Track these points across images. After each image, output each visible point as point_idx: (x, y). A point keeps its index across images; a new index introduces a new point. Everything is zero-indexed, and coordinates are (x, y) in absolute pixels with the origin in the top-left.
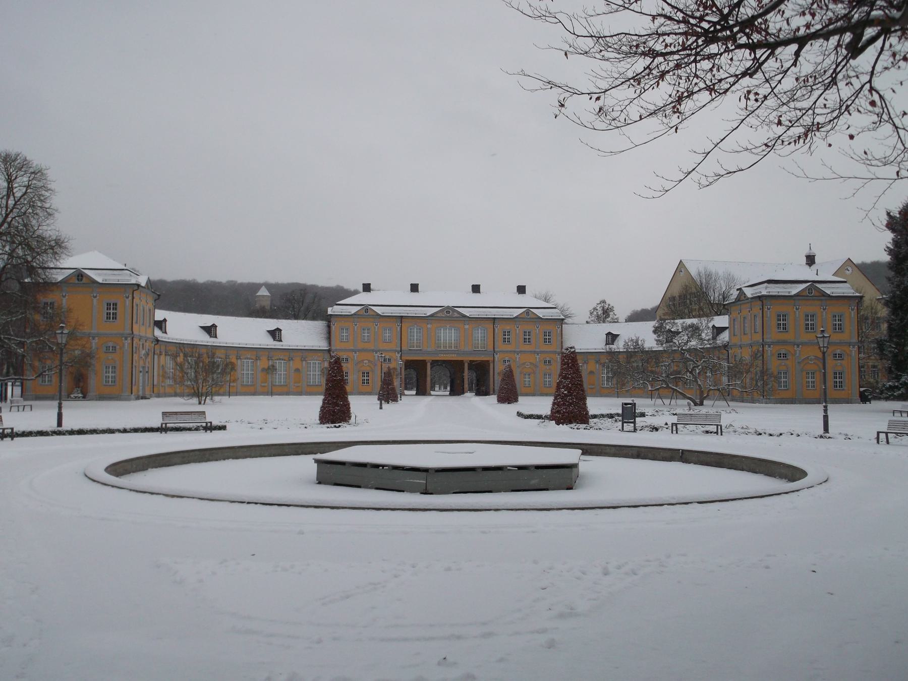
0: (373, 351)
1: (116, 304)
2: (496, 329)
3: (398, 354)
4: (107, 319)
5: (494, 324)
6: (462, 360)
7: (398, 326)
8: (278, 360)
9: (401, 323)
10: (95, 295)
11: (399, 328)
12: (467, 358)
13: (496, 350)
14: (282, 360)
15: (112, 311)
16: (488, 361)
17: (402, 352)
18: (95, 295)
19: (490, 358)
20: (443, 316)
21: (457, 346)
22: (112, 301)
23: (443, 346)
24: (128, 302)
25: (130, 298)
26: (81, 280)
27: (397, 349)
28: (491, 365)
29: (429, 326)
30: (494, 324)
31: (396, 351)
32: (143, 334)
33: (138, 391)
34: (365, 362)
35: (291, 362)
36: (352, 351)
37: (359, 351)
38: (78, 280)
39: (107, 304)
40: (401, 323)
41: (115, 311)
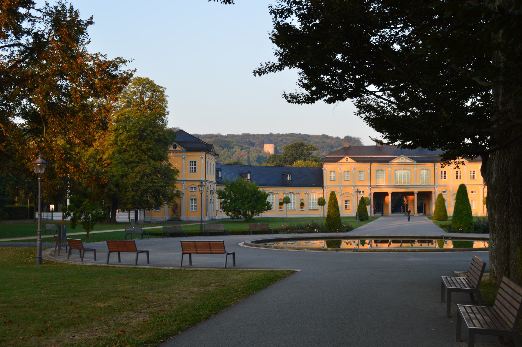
1: (195, 162)
3: (369, 188)
4: (191, 171)
5: (434, 167)
6: (413, 192)
8: (289, 193)
9: (370, 167)
10: (184, 157)
12: (416, 191)
13: (436, 184)
14: (292, 193)
15: (193, 166)
16: (430, 193)
17: (372, 187)
18: (184, 157)
20: (399, 162)
21: (409, 182)
22: (193, 160)
23: (400, 183)
24: (203, 161)
25: (204, 158)
26: (176, 148)
28: (433, 195)
29: (389, 169)
30: (434, 167)
32: (210, 180)
33: (209, 215)
34: (347, 194)
35: (298, 195)
36: (338, 186)
37: (342, 186)
38: (174, 148)
39: (191, 162)
40: (370, 167)
41: (195, 166)
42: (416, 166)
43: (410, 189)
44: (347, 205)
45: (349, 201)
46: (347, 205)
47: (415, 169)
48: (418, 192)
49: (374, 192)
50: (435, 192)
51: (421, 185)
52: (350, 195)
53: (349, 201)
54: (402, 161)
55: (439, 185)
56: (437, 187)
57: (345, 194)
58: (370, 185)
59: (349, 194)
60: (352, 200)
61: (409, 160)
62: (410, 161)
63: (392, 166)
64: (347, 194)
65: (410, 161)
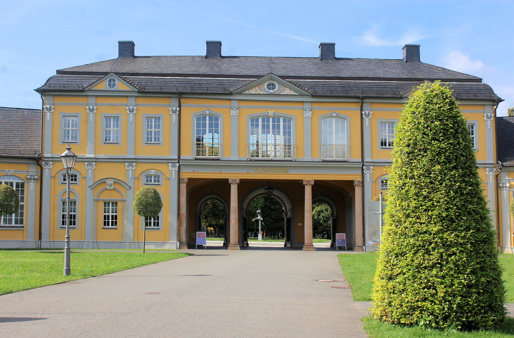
0: (123, 160)
2: (366, 121)
3: (174, 166)
5: (362, 110)
7: (174, 112)
9: (180, 106)
11: (175, 117)
13: (366, 160)
16: (350, 184)
19: (354, 176)
27: (171, 157)
29: (234, 112)
30: (362, 110)
31: (168, 161)
34: (110, 182)
40: (180, 106)
42: (307, 106)
43: (292, 171)
44: (110, 214)
45: (115, 204)
46: (110, 214)
47: (309, 114)
48: (316, 182)
49: (189, 179)
50: (363, 182)
51: (324, 161)
52: (117, 187)
53: (115, 204)
54: (271, 91)
55: (375, 164)
56: (368, 169)
57: (103, 182)
58: (176, 157)
59: (117, 182)
60: (122, 201)
61: (291, 89)
62: (292, 93)
63: (242, 104)
64: (110, 182)
65: (292, 93)
